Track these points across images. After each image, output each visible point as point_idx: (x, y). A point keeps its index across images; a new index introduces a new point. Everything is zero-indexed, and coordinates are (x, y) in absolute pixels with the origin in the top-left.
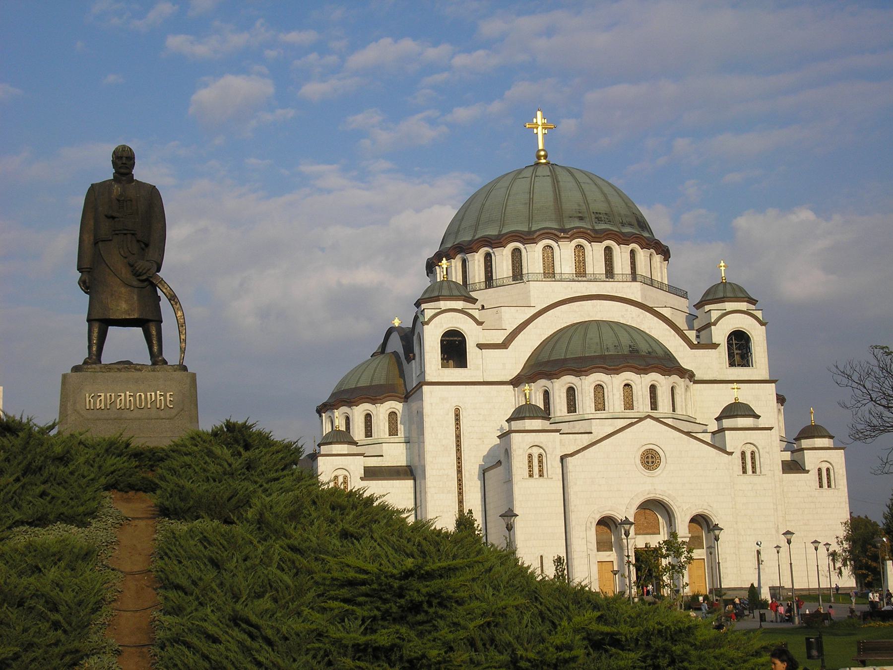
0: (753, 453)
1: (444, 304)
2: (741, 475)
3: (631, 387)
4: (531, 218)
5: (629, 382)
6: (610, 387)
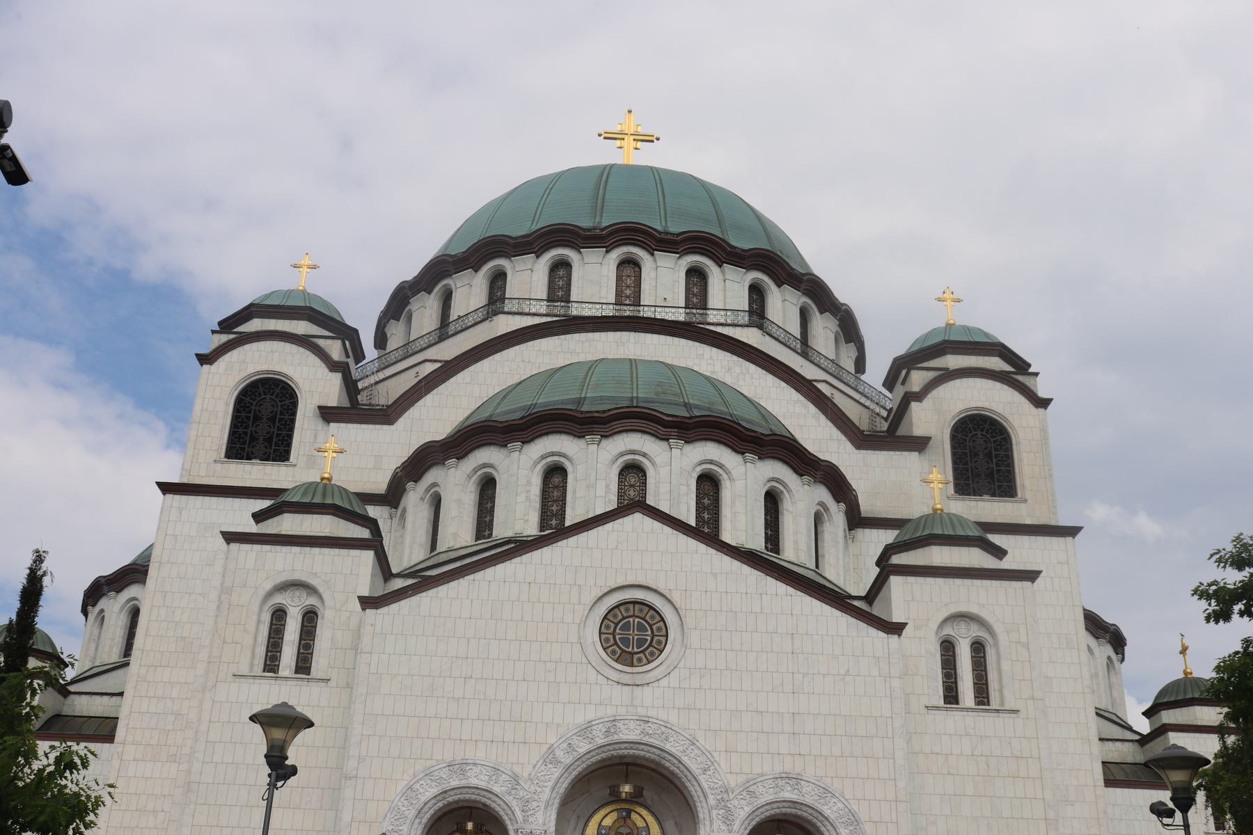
0: (978, 648)
1: (255, 325)
2: (937, 708)
3: (645, 475)
5: (637, 457)
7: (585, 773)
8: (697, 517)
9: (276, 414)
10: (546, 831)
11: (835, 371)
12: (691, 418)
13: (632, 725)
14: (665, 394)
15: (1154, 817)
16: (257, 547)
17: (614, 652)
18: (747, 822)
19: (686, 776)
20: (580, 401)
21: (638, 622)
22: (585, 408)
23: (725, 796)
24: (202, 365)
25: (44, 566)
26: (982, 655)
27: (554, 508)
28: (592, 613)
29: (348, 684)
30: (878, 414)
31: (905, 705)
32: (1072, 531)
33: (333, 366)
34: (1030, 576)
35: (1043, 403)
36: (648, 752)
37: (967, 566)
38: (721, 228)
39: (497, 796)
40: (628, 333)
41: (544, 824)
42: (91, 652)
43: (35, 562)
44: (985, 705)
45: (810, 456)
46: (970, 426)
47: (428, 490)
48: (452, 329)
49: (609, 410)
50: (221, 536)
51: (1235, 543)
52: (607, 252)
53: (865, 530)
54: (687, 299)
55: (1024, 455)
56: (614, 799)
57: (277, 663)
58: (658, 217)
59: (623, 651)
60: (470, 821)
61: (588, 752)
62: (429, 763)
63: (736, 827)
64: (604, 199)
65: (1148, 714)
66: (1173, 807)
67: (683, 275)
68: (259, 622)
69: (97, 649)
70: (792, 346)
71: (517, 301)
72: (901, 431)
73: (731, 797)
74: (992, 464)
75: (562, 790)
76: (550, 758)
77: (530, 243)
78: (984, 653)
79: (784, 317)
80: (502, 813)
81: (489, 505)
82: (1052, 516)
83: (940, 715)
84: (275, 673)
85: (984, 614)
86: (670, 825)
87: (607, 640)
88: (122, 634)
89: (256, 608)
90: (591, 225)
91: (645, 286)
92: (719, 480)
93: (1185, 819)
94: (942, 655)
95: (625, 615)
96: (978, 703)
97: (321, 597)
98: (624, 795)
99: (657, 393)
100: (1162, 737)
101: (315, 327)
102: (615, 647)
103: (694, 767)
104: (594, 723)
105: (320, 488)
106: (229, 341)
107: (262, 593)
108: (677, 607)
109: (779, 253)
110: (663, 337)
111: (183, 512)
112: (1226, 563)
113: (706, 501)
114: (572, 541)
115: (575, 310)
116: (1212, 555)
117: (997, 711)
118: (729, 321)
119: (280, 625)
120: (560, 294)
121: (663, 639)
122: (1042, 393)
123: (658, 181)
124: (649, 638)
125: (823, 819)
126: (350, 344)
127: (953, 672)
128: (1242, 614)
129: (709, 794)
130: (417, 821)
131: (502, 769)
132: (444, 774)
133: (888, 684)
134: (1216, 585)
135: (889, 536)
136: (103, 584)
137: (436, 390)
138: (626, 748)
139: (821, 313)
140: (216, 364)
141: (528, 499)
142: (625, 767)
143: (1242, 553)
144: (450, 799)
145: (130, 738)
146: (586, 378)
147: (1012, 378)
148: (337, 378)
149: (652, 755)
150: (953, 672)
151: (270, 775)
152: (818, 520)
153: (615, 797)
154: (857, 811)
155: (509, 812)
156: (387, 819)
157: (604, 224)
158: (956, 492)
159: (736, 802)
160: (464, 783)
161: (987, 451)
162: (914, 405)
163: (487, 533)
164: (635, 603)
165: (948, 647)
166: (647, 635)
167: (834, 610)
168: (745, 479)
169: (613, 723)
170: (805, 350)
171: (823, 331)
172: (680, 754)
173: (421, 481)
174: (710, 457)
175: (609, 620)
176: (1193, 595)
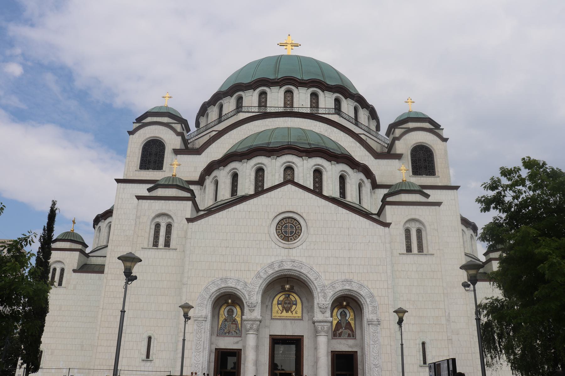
0: (419, 231)
1: (149, 119)
2: (403, 254)
3: (294, 171)
4: (254, 76)
5: (290, 164)
6: (269, 169)
7: (272, 281)
8: (313, 186)
9: (157, 153)
10: (257, 302)
11: (369, 131)
12: (311, 148)
13: (289, 263)
14: (300, 139)
15: (463, 287)
16: (149, 201)
17: (281, 236)
18: (332, 298)
19: (309, 281)
20: (269, 143)
21: (291, 225)
22: (271, 146)
23: (324, 288)
24: (130, 135)
25: (56, 206)
26: (420, 234)
27: (260, 184)
28: (273, 222)
29: (184, 250)
30: (384, 146)
31: (391, 253)
32: (456, 188)
33: (178, 134)
34: (438, 204)
35: (445, 140)
36: (295, 273)
37: (415, 201)
38: (323, 77)
39: (239, 290)
40: (288, 118)
41: (257, 300)
42: (97, 242)
43: (53, 205)
44: (421, 252)
45: (356, 161)
46: (418, 149)
47: (213, 179)
48: (223, 118)
49: (280, 146)
50: (135, 197)
51: (491, 180)
52: (280, 88)
53: (379, 189)
54: (311, 105)
55: (438, 160)
56: (284, 290)
57: (158, 243)
58: (299, 74)
59: (285, 236)
60: (230, 299)
61: (272, 274)
62: (214, 279)
63: (328, 300)
64: (279, 68)
65: (485, 254)
66: (470, 284)
67: (309, 95)
68: (150, 228)
69: (99, 240)
70: (351, 121)
71: (247, 107)
72: (392, 152)
73: (326, 288)
74: (426, 163)
75: (263, 288)
76: (258, 276)
77: (251, 85)
78: (421, 233)
79: (348, 110)
80: (241, 296)
81: (236, 184)
82: (449, 182)
83: (405, 257)
84: (157, 247)
85: (421, 219)
86: (304, 300)
87: (279, 232)
88: (107, 235)
89: (149, 223)
90: (274, 78)
91: (295, 100)
92: (322, 172)
93: (474, 288)
94: (405, 234)
95: (285, 222)
96: (419, 252)
97: (172, 219)
98: (287, 289)
99: (298, 140)
100: (490, 263)
101: (171, 119)
102: (282, 235)
103: (312, 278)
104: (274, 263)
105: (172, 178)
106: (139, 126)
107: (151, 218)
108: (305, 219)
109: (346, 87)
110: (301, 119)
111: (125, 190)
112: (488, 188)
113: (317, 180)
114: (265, 195)
115: (269, 110)
116: (482, 185)
117: (426, 254)
118: (327, 113)
119: (157, 229)
120: (263, 104)
121: (300, 231)
122: (445, 136)
123: (299, 61)
124: (295, 231)
125: (360, 296)
126: (184, 125)
127: (409, 241)
128: (494, 208)
129: (318, 288)
130: (210, 299)
131: (240, 280)
132: (219, 282)
133: (384, 246)
134: (484, 197)
135: (386, 191)
136: (99, 217)
137: (216, 141)
138: (286, 272)
139: (362, 109)
140: (135, 135)
141: (250, 181)
142: (287, 279)
143: (494, 184)
144: (222, 291)
145: (109, 272)
146: (271, 135)
147: (433, 131)
148: (179, 139)
149: (296, 274)
150: (409, 241)
151: (126, 279)
152: (360, 186)
153: (283, 290)
154: (373, 292)
155: (244, 296)
156: (199, 298)
157: (279, 77)
158: (413, 174)
159: (328, 291)
160: (226, 285)
161: (424, 159)
162: (397, 142)
163: (235, 194)
164: (289, 218)
165: (408, 232)
166: (294, 230)
167: (364, 219)
168: (332, 171)
169: (282, 263)
170: (356, 122)
171: (363, 115)
172: (306, 273)
173: (210, 176)
174: (318, 163)
175: (280, 225)
176: (476, 202)
